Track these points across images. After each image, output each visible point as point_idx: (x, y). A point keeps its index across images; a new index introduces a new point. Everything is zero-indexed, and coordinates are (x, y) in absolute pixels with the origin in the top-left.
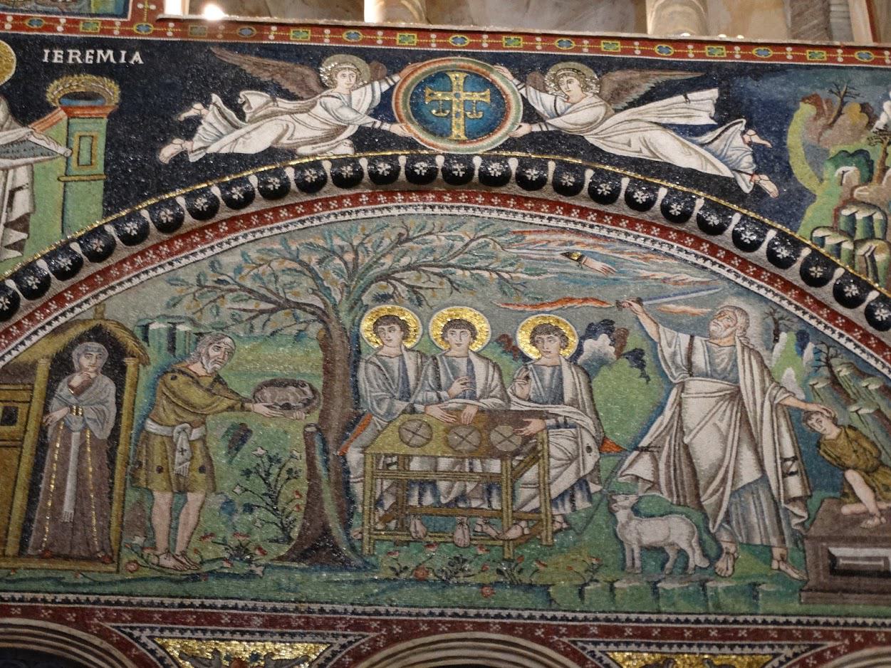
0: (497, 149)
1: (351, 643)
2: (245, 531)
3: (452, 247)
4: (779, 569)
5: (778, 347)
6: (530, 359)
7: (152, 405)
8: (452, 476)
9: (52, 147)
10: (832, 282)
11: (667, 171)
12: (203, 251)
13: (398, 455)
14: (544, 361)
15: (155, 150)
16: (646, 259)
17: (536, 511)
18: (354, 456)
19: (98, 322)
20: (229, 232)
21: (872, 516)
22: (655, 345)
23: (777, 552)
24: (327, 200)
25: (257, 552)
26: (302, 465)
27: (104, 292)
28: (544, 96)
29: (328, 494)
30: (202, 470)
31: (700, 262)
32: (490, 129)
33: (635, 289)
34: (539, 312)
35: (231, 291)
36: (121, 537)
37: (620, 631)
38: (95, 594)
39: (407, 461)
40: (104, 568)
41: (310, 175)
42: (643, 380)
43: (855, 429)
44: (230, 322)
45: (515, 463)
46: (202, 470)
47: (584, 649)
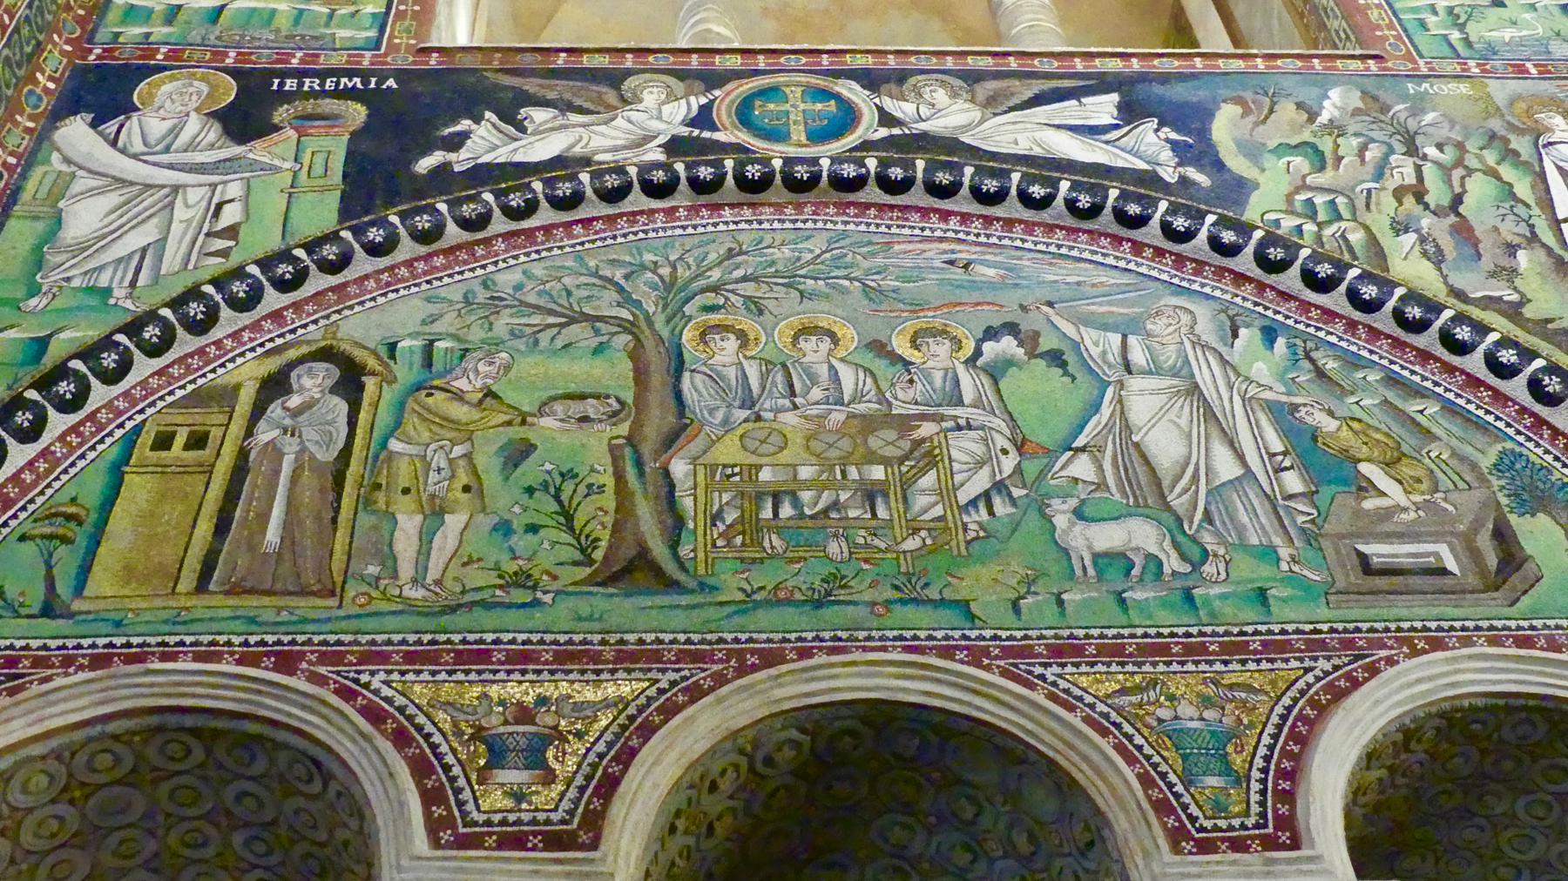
0: (851, 150)
3: (799, 259)
4: (1291, 571)
7: (398, 424)
8: (819, 486)
9: (277, 162)
10: (1299, 262)
11: (1068, 166)
13: (741, 465)
14: (930, 364)
17: (942, 519)
18: (679, 468)
19: (329, 342)
21: (1405, 510)
22: (1076, 346)
23: (1284, 552)
24: (634, 214)
25: (545, 577)
26: (609, 480)
27: (338, 312)
28: (903, 104)
30: (466, 489)
31: (1122, 264)
35: (507, 306)
36: (348, 566)
37: (1078, 651)
38: (304, 633)
39: (753, 471)
40: (319, 602)
41: (612, 181)
42: (1067, 380)
43: (1360, 421)
44: (507, 337)
46: (466, 489)
47: (1030, 673)
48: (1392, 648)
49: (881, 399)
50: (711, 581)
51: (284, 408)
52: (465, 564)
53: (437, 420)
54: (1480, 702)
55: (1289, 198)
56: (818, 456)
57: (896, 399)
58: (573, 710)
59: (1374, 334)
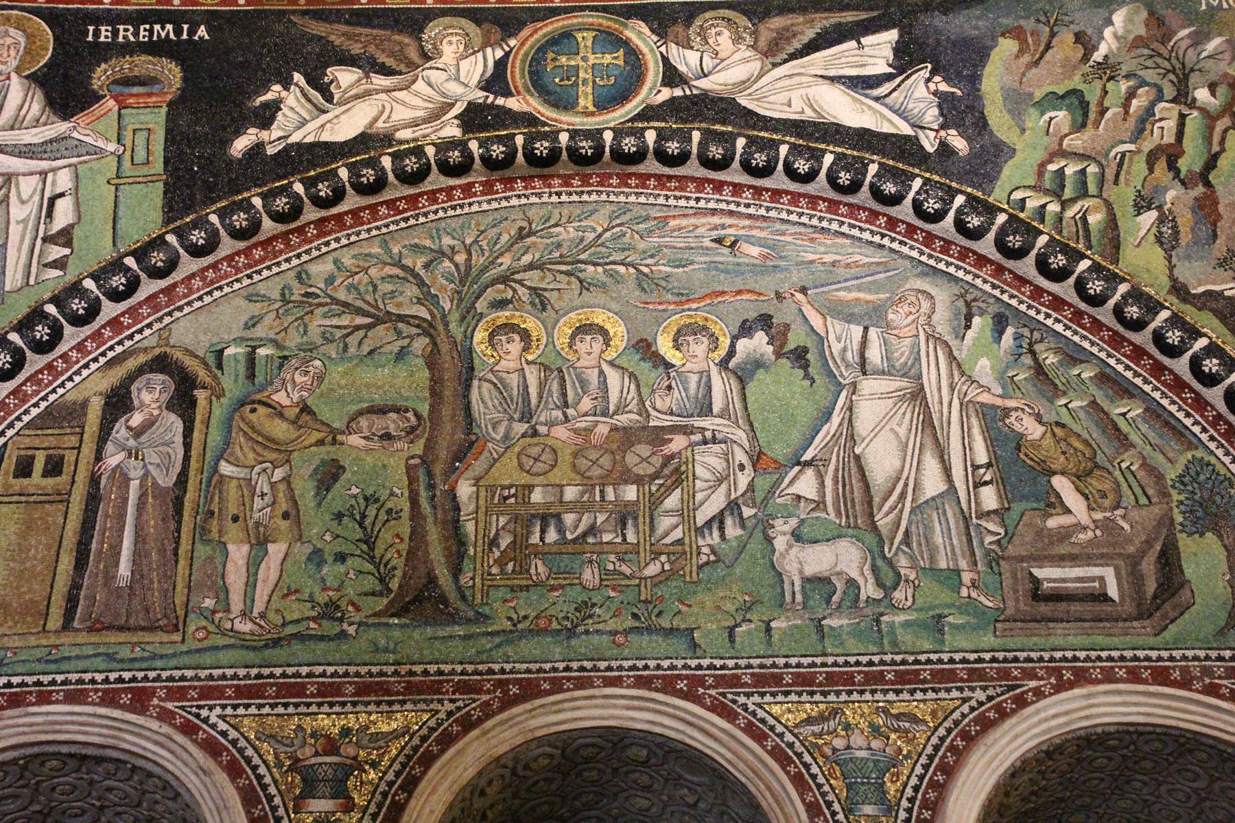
0: (632, 120)
1: (459, 709)
2: (336, 585)
3: (582, 240)
4: (969, 597)
5: (970, 334)
6: (673, 366)
8: (579, 507)
9: (100, 143)
10: (1035, 251)
11: (834, 132)
12: (288, 260)
13: (517, 486)
14: (689, 366)
15: (226, 143)
16: (812, 240)
17: (679, 542)
18: (465, 490)
19: (163, 350)
20: (318, 237)
21: (1085, 528)
23: (967, 577)
24: (434, 192)
25: (350, 608)
27: (170, 314)
28: (688, 53)
29: (433, 534)
30: (286, 516)
31: (877, 239)
32: (621, 96)
33: (797, 277)
34: (683, 310)
36: (188, 600)
37: (777, 679)
40: (166, 638)
41: (411, 164)
42: (808, 383)
43: (1063, 426)
44: (320, 341)
45: (654, 488)
46: (286, 516)
47: (734, 702)
48: (1042, 679)
49: (643, 411)
50: (487, 610)
51: (128, 427)
52: (285, 596)
53: (260, 439)
54: (1112, 729)
55: (1041, 173)
56: (582, 475)
57: (654, 408)
58: (369, 741)
59: (1097, 326)
